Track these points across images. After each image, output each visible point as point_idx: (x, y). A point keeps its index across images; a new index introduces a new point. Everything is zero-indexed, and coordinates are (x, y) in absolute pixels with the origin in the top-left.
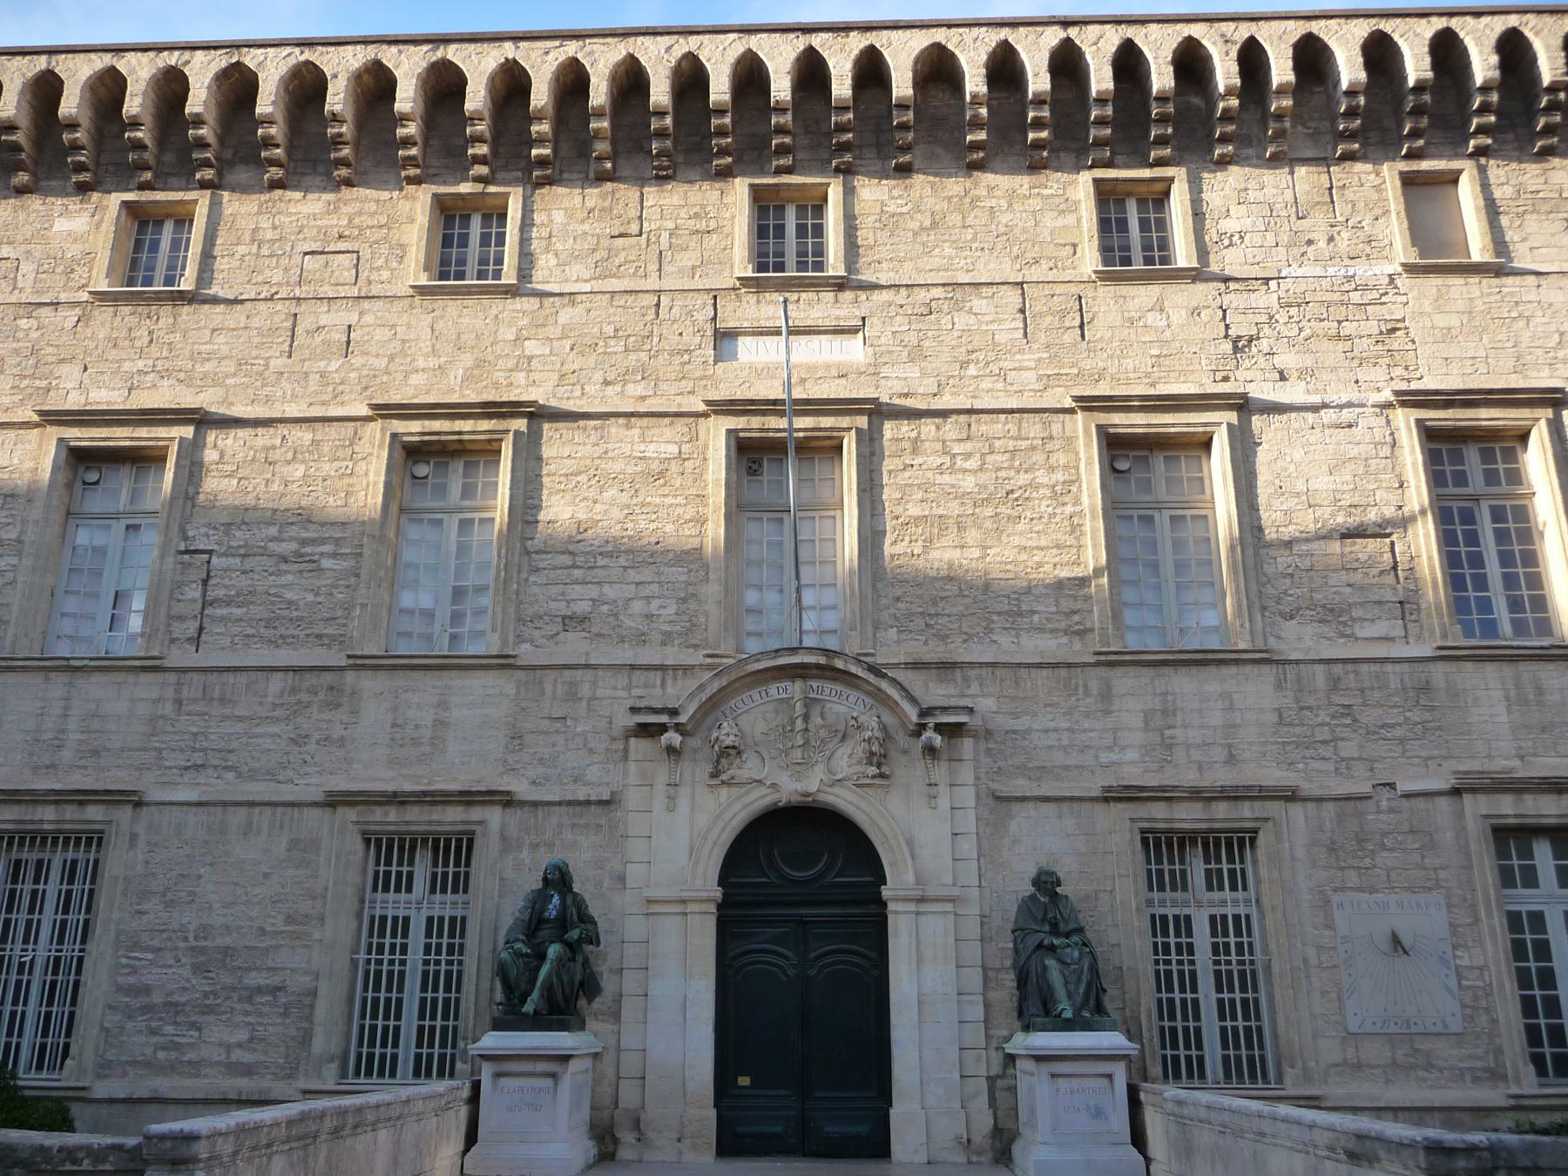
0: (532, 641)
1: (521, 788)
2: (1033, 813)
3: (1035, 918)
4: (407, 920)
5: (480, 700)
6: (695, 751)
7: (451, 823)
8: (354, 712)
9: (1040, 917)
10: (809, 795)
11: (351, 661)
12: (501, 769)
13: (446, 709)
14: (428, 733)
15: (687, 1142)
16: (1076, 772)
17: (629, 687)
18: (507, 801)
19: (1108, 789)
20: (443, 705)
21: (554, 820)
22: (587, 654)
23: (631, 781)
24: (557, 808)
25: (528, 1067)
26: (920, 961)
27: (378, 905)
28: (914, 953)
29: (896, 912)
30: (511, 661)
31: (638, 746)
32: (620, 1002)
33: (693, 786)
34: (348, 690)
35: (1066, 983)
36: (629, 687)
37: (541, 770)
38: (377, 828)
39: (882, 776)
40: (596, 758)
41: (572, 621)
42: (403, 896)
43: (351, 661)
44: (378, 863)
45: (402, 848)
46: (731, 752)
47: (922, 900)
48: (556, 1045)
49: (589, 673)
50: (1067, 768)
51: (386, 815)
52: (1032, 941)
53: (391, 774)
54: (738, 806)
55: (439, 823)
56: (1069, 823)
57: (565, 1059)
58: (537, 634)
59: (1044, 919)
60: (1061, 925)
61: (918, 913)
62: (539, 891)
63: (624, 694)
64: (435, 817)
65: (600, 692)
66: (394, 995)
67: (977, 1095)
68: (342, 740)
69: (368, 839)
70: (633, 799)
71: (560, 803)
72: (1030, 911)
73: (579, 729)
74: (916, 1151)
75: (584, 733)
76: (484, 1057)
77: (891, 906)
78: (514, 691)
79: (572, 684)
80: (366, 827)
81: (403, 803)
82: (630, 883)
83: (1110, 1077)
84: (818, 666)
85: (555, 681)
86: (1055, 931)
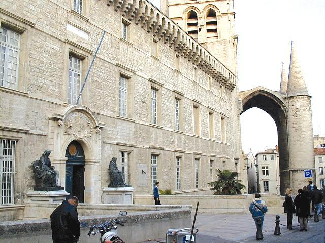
5: (20, 104)
18: (26, 132)
20: (11, 104)
23: (50, 131)
41: (39, 88)
63: (48, 109)
79: (38, 104)
84: (83, 110)
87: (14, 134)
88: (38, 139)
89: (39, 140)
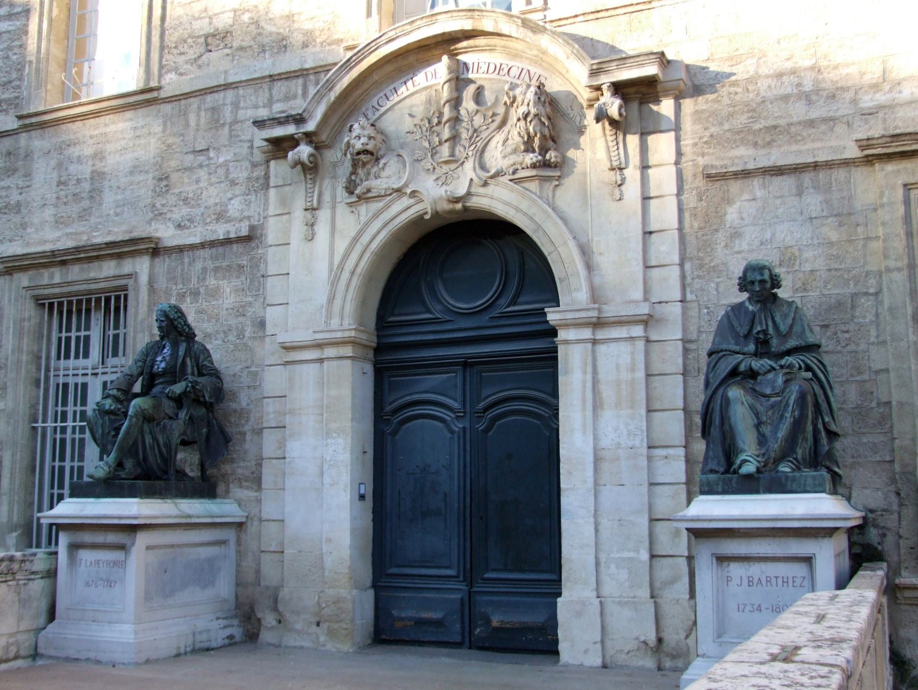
0: (176, 70)
1: (168, 235)
2: (759, 193)
3: (736, 335)
4: (85, 386)
6: (335, 165)
7: (106, 279)
8: (28, 175)
9: (743, 331)
10: (457, 200)
11: (21, 123)
12: (151, 215)
13: (103, 158)
14: (86, 186)
15: (324, 626)
16: (823, 127)
17: (270, 102)
18: (156, 250)
19: (864, 144)
21: (199, 265)
22: (226, 72)
23: (272, 210)
24: (201, 253)
25: (100, 538)
26: (597, 405)
27: (62, 373)
28: (589, 395)
29: (566, 342)
30: (155, 94)
31: (279, 169)
32: (260, 465)
33: (333, 208)
34: (22, 152)
35: (758, 425)
36: (270, 102)
37: (185, 211)
38: (46, 292)
39: (546, 164)
40: (238, 190)
42: (81, 362)
43: (21, 123)
44: (61, 331)
45: (79, 311)
46: (367, 158)
47: (598, 324)
48: (126, 513)
49: (230, 95)
50: (811, 123)
51: (52, 276)
52: (725, 366)
53: (58, 234)
54: (377, 224)
55: (95, 280)
56: (813, 202)
57: (133, 529)
58: (181, 59)
59: (746, 337)
60: (774, 342)
61: (595, 342)
62: (157, 342)
64: (92, 275)
65: (241, 114)
66: (57, 464)
67: (673, 581)
68: (19, 204)
69: (40, 302)
70: (272, 233)
71: (202, 245)
72: (732, 326)
73: (221, 160)
74: (586, 652)
75: (226, 164)
76: (61, 527)
77: (562, 335)
78: (160, 129)
79: (214, 109)
80: (37, 292)
81: (63, 263)
82: (270, 330)
83: (808, 560)
85: (199, 108)
86: (763, 348)
87: (109, 268)
88: (210, 265)
89: (216, 270)
